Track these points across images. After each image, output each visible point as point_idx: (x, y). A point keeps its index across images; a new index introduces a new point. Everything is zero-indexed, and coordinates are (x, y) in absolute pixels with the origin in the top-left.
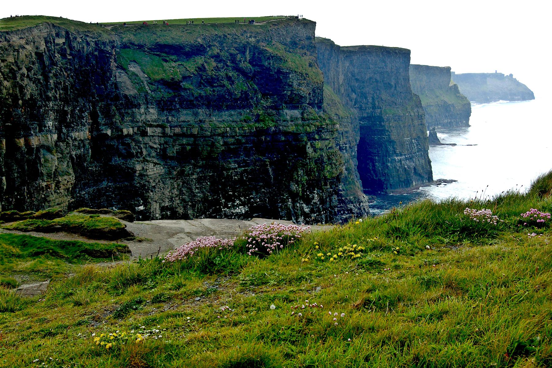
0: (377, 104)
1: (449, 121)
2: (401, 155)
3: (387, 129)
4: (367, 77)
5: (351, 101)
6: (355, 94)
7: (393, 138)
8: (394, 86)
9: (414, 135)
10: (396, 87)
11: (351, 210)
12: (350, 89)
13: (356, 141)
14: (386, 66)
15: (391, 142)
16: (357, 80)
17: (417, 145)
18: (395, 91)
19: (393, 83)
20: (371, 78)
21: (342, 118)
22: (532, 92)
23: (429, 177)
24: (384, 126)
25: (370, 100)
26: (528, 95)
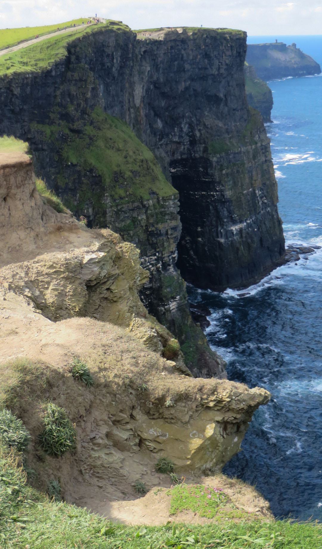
0: (198, 134)
2: (241, 222)
3: (218, 180)
4: (182, 86)
5: (155, 134)
6: (162, 121)
7: (228, 194)
8: (224, 99)
10: (226, 100)
14: (211, 65)
15: (223, 201)
16: (164, 95)
17: (261, 198)
18: (226, 109)
19: (221, 95)
20: (187, 89)
21: (164, 200)
22: (318, 65)
24: (212, 175)
25: (185, 129)
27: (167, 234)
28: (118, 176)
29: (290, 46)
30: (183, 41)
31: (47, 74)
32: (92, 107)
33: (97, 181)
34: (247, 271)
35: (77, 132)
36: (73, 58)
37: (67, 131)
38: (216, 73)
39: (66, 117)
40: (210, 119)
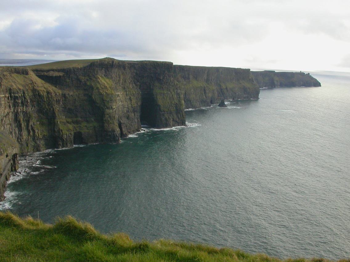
0: (152, 87)
1: (247, 96)
6: (139, 82)
9: (173, 102)
11: (110, 135)
12: (136, 80)
13: (137, 104)
19: (161, 78)
23: (183, 123)
26: (317, 84)
27: (108, 101)
28: (98, 88)
29: (307, 74)
30: (146, 64)
31: (85, 67)
32: (96, 74)
33: (93, 88)
34: (164, 125)
35: (91, 79)
36: (92, 65)
37: (88, 78)
38: (159, 72)
39: (89, 76)
40: (157, 84)
